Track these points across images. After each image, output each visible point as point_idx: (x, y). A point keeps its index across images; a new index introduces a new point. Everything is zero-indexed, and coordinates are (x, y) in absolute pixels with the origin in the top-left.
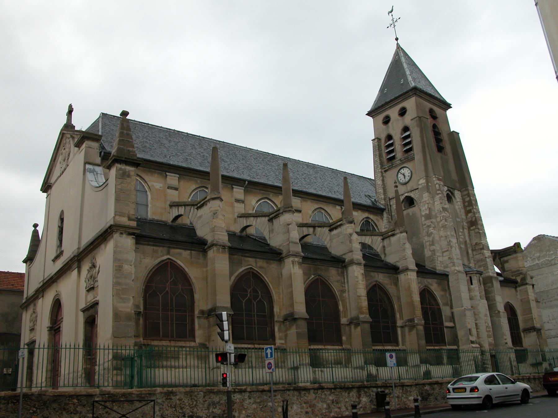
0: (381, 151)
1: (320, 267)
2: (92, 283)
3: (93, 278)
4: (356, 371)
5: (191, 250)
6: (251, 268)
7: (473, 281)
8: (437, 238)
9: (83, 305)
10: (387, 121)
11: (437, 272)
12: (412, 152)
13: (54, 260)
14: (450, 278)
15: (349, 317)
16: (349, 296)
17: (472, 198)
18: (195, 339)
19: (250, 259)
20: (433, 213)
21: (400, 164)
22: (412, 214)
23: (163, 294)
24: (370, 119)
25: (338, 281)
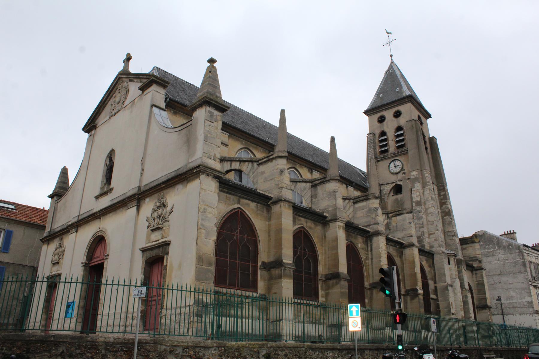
0: (375, 144)
1: (351, 234)
2: (160, 222)
3: (163, 218)
4: (376, 331)
5: (257, 202)
6: (303, 227)
7: (451, 262)
8: (425, 222)
9: (144, 244)
10: (382, 120)
11: (426, 250)
12: (404, 148)
13: (97, 198)
14: (436, 257)
15: (371, 282)
16: (372, 263)
17: (446, 193)
18: (257, 290)
19: (302, 219)
20: (423, 201)
21: (393, 157)
22: (401, 200)
23: (231, 242)
24: (366, 118)
25: (363, 249)
